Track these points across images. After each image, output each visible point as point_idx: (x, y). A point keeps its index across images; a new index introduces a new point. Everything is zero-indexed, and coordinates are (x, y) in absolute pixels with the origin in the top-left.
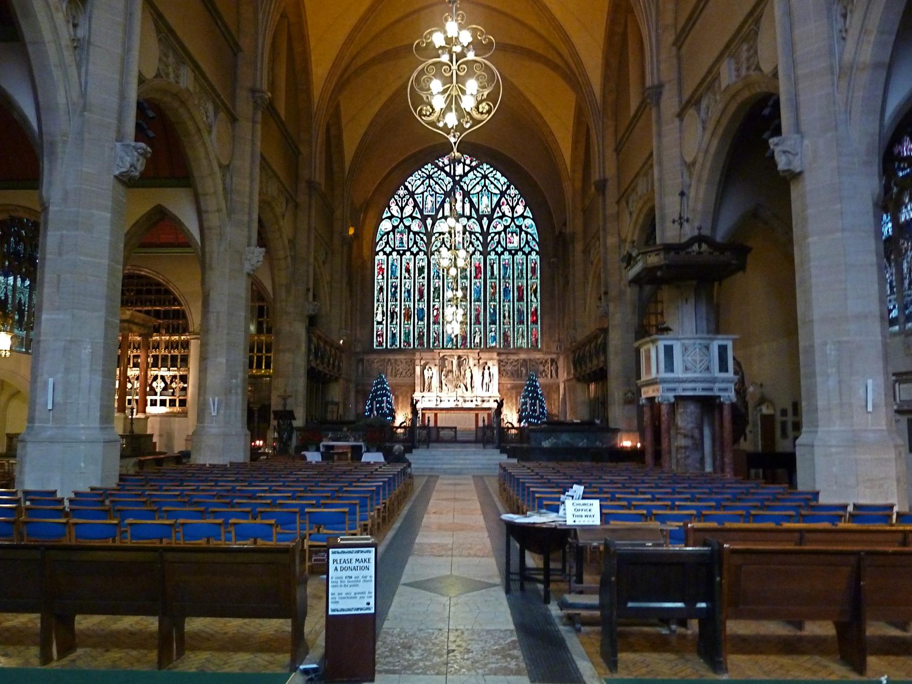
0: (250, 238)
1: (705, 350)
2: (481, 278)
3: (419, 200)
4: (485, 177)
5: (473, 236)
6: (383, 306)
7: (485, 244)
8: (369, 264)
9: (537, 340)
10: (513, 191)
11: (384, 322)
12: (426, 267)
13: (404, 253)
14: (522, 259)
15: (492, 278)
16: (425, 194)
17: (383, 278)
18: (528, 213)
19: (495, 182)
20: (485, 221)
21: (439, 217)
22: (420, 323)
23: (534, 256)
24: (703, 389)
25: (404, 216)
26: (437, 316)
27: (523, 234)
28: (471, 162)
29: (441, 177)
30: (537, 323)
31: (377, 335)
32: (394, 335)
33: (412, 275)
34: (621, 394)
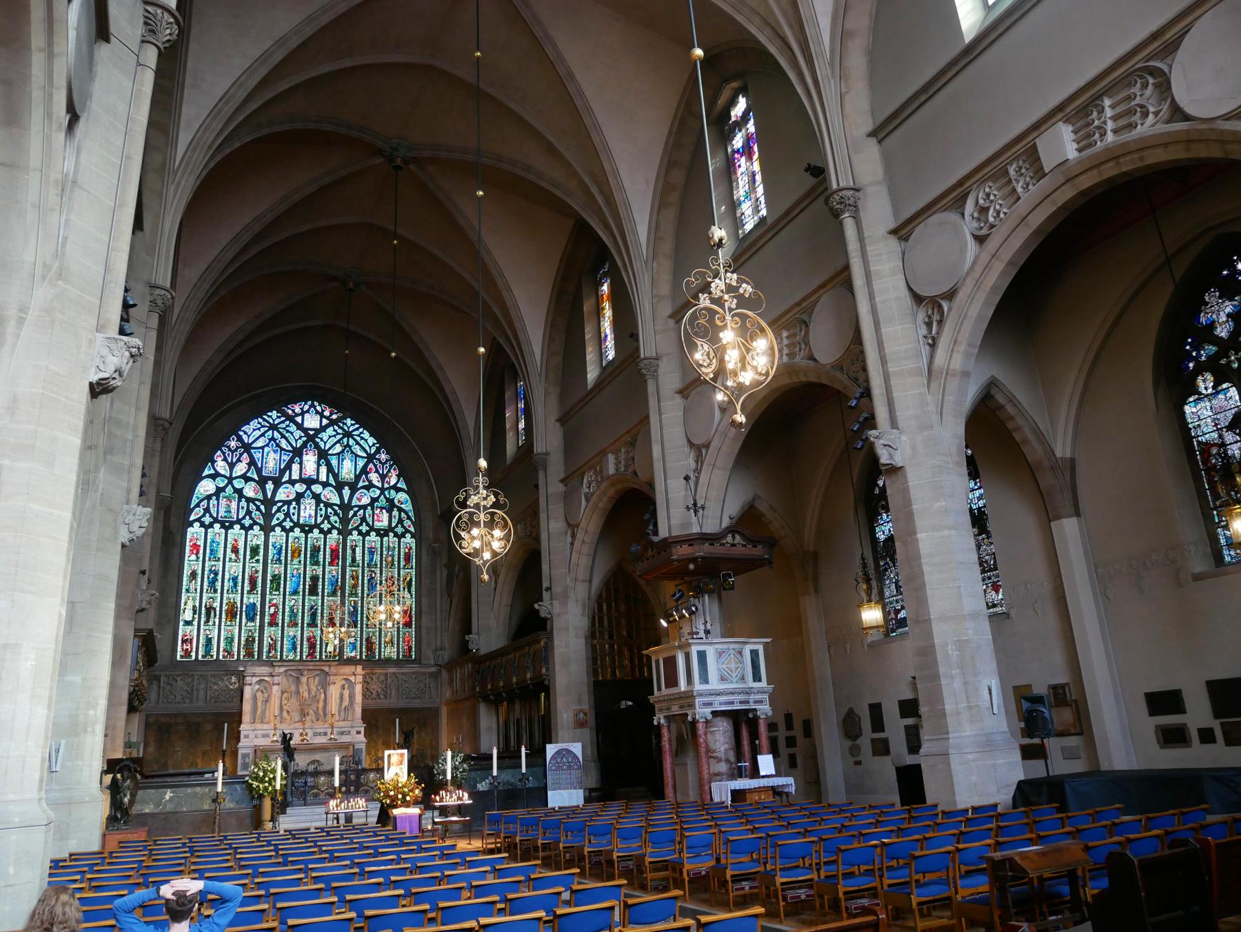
0: (129, 492)
1: (739, 656)
2: (338, 565)
3: (257, 455)
4: (348, 434)
6: (194, 599)
7: (345, 521)
8: (178, 539)
9: (410, 648)
10: (383, 457)
11: (195, 623)
12: (262, 547)
13: (231, 527)
16: (266, 449)
17: (198, 558)
18: (402, 485)
19: (362, 442)
20: (346, 492)
21: (284, 480)
22: (249, 624)
23: (408, 539)
24: (741, 702)
25: (234, 475)
26: (273, 616)
27: (395, 513)
28: (331, 414)
29: (290, 429)
31: (184, 641)
32: (209, 641)
34: (571, 715)
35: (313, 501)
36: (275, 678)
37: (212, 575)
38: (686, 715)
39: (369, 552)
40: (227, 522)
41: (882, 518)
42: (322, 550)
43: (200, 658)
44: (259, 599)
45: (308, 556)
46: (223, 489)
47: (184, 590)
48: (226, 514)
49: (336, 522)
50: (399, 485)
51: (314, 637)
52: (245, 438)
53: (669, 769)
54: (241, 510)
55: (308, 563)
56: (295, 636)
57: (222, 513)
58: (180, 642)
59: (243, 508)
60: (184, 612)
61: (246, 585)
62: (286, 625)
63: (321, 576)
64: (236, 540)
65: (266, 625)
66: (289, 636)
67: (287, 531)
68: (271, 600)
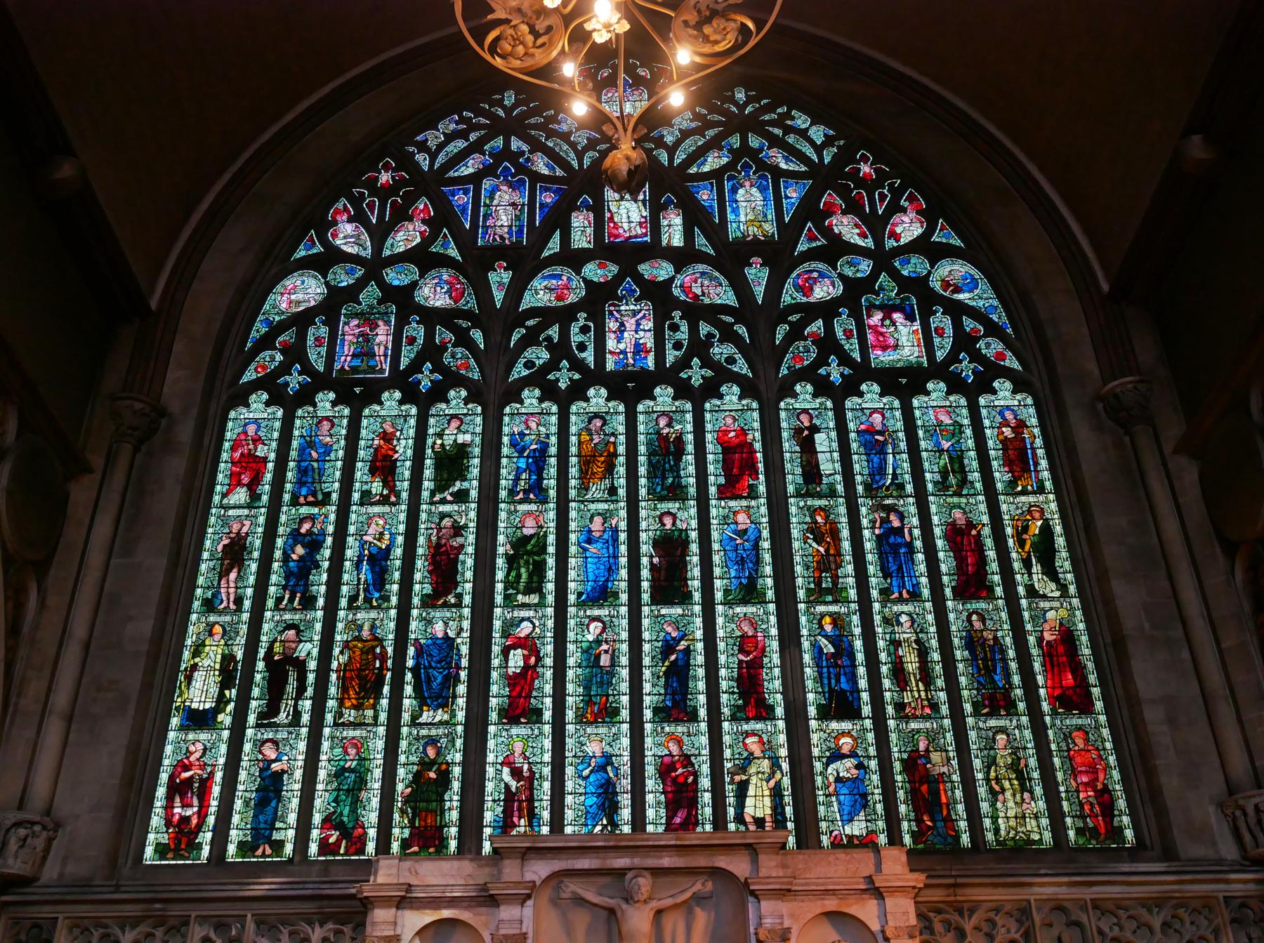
2: (753, 495)
3: (461, 199)
5: (704, 328)
8: (185, 432)
9: (1105, 798)
11: (225, 719)
14: (950, 409)
15: (808, 494)
16: (487, 184)
17: (255, 496)
19: (791, 139)
21: (546, 253)
25: (387, 253)
26: (522, 683)
27: (940, 320)
30: (1086, 708)
31: (178, 789)
32: (271, 786)
33: (404, 486)
35: (646, 307)
36: (507, 912)
37: (300, 550)
39: (864, 444)
40: (359, 382)
42: (690, 448)
43: (232, 849)
44: (466, 624)
45: (642, 470)
46: (351, 294)
47: (196, 604)
48: (357, 362)
49: (731, 360)
50: (935, 238)
51: (686, 760)
52: (423, 160)
54: (405, 350)
55: (643, 492)
56: (608, 759)
57: (345, 359)
58: (161, 792)
59: (412, 341)
60: (189, 679)
61: (418, 576)
62: (570, 715)
63: (694, 535)
64: (387, 437)
65: (494, 716)
66: (585, 759)
67: (565, 399)
68: (509, 625)
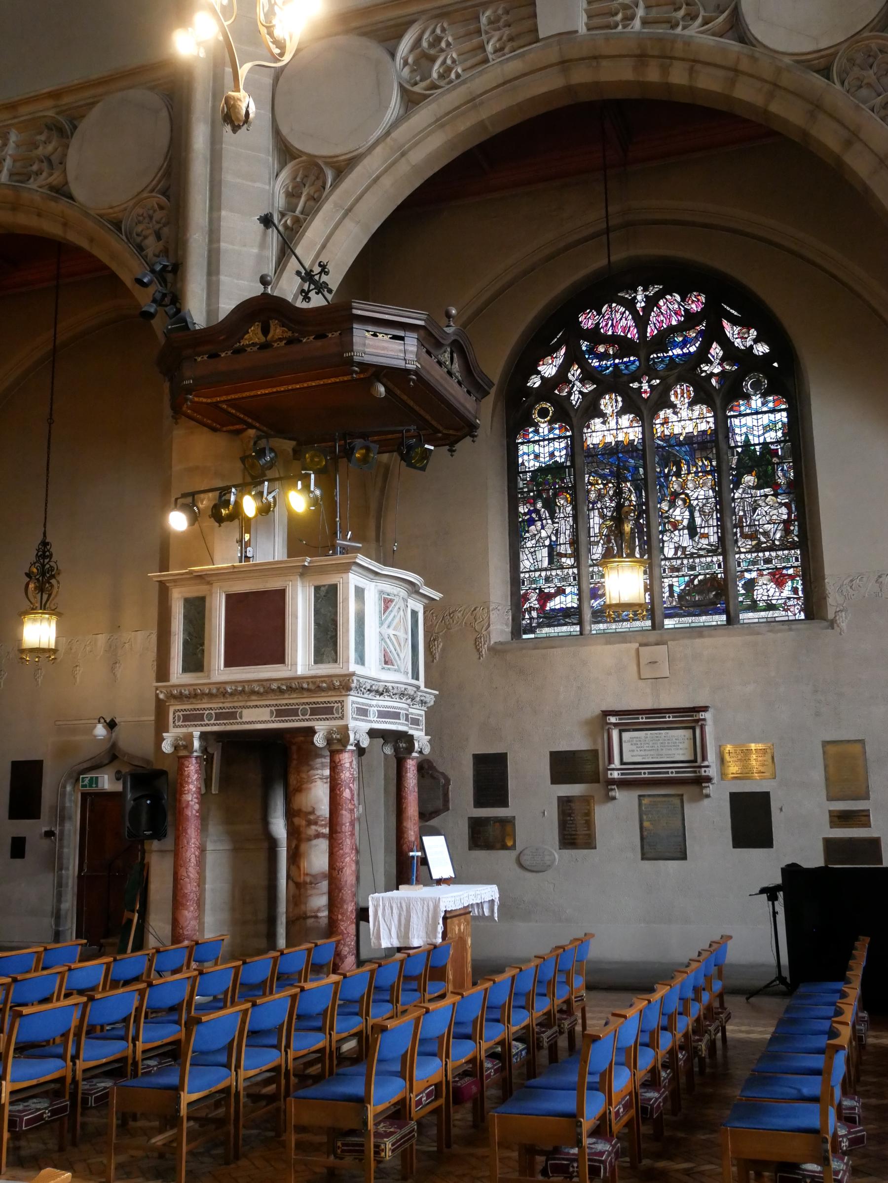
38: (311, 731)
41: (536, 432)
53: (193, 860)
